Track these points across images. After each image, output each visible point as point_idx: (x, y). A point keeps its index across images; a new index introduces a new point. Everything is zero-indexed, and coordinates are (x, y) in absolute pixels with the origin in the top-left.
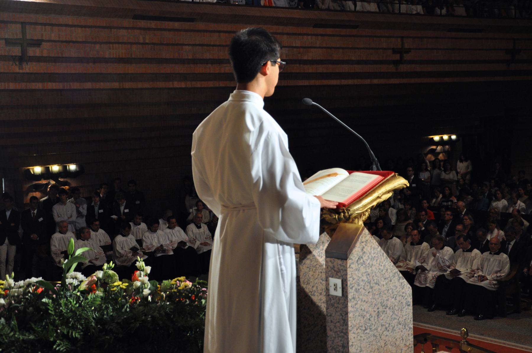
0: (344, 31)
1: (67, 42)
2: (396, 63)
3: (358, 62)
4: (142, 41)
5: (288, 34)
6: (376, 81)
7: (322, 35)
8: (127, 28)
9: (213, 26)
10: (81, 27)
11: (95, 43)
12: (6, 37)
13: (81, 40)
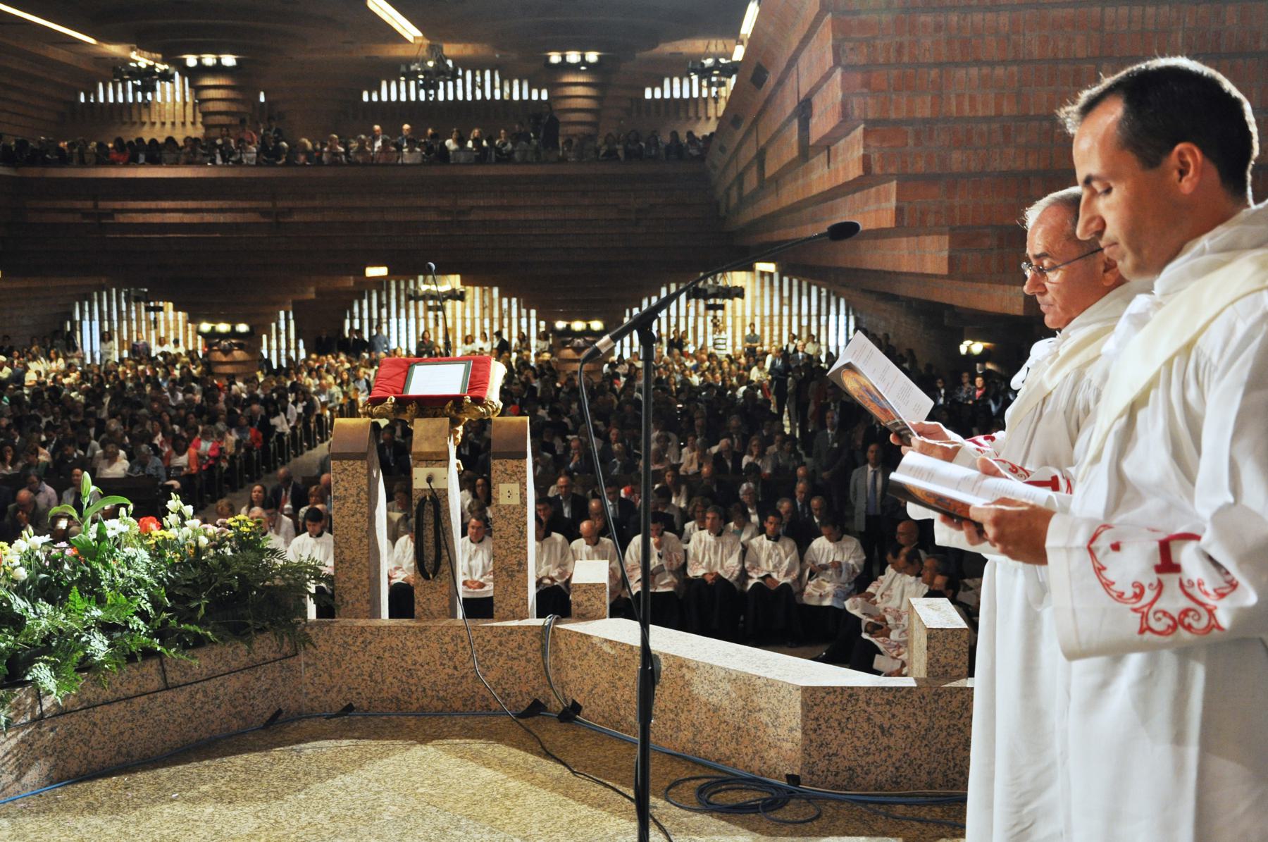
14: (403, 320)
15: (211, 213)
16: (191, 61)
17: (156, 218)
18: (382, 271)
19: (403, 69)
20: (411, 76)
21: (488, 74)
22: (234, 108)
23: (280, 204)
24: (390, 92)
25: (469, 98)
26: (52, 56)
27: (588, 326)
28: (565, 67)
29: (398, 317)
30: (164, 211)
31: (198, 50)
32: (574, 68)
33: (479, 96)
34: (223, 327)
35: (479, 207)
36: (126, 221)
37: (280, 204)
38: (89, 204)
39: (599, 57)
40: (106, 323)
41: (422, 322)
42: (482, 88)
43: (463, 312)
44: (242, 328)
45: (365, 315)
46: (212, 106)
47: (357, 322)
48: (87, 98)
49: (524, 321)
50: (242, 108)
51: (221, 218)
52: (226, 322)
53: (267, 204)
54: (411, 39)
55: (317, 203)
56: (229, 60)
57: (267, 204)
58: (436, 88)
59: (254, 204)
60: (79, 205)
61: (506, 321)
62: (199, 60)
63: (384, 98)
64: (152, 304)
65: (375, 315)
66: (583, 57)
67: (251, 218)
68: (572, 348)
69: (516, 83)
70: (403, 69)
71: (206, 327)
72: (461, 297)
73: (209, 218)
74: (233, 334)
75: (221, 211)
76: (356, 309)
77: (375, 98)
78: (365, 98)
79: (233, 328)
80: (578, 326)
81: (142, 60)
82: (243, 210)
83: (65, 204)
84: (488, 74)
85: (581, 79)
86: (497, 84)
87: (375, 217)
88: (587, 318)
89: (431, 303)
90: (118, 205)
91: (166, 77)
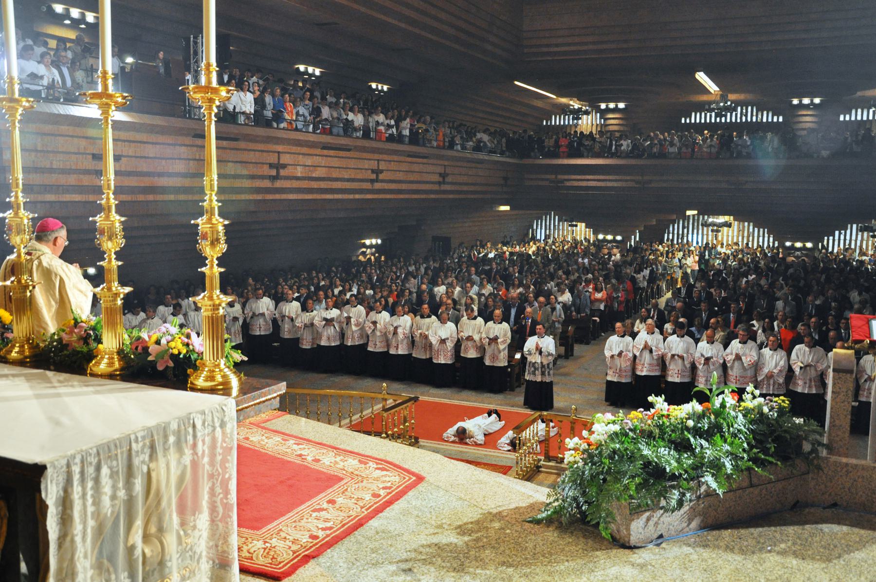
0: (341, 153)
1: (141, 157)
2: (372, 181)
3: (348, 180)
4: (197, 157)
5: (303, 154)
6: (357, 196)
7: (326, 156)
8: (187, 146)
9: (252, 146)
10: (153, 143)
11: (163, 159)
12: (95, 152)
13: (151, 155)
14: (695, 235)
15: (611, 182)
16: (603, 106)
17: (584, 184)
18: (696, 212)
19: (707, 107)
20: (711, 110)
21: (750, 108)
22: (622, 128)
23: (646, 178)
24: (696, 118)
25: (739, 121)
26: (535, 104)
27: (804, 245)
28: (801, 106)
29: (693, 234)
30: (588, 180)
32: (807, 107)
33: (744, 120)
34: (610, 237)
37: (646, 178)
38: (553, 176)
41: (705, 237)
42: (746, 116)
43: (728, 233)
44: (619, 238)
45: (676, 232)
46: (611, 128)
47: (671, 236)
48: (547, 123)
49: (761, 239)
50: (626, 129)
51: (615, 184)
54: (712, 92)
56: (621, 105)
58: (726, 116)
60: (548, 177)
61: (751, 238)
62: (607, 106)
63: (693, 121)
65: (681, 232)
66: (812, 101)
67: (630, 184)
68: (794, 257)
69: (765, 113)
70: (707, 107)
72: (729, 225)
73: (609, 184)
74: (614, 241)
76: (671, 229)
77: (688, 121)
78: (683, 121)
80: (798, 245)
81: (576, 105)
82: (627, 181)
83: (543, 176)
84: (750, 108)
85: (809, 113)
86: (755, 114)
88: (804, 241)
89: (715, 228)
90: (566, 177)
91: (587, 113)
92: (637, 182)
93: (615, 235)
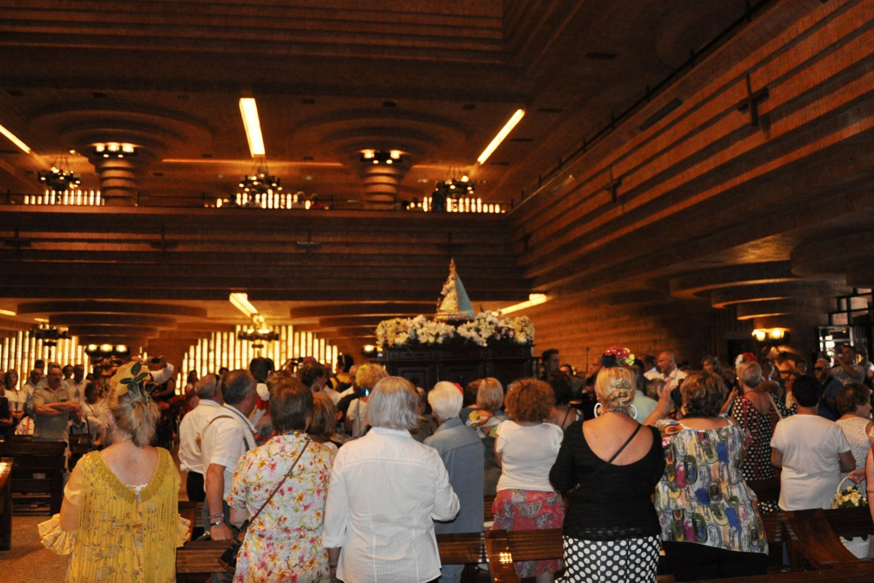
22: (127, 184)
23: (167, 237)
31: (105, 139)
34: (107, 348)
35: (329, 243)
36: (40, 248)
38: (12, 234)
39: (401, 156)
40: (13, 361)
44: (121, 348)
46: (111, 183)
47: (192, 362)
50: (133, 185)
51: (118, 247)
52: (109, 343)
53: (158, 237)
55: (198, 237)
56: (128, 148)
57: (158, 237)
59: (146, 236)
64: (47, 341)
65: (205, 357)
71: (93, 347)
73: (109, 247)
74: (114, 352)
75: (119, 241)
79: (114, 348)
87: (244, 249)
90: (34, 235)
92: (154, 243)
93: (115, 343)
